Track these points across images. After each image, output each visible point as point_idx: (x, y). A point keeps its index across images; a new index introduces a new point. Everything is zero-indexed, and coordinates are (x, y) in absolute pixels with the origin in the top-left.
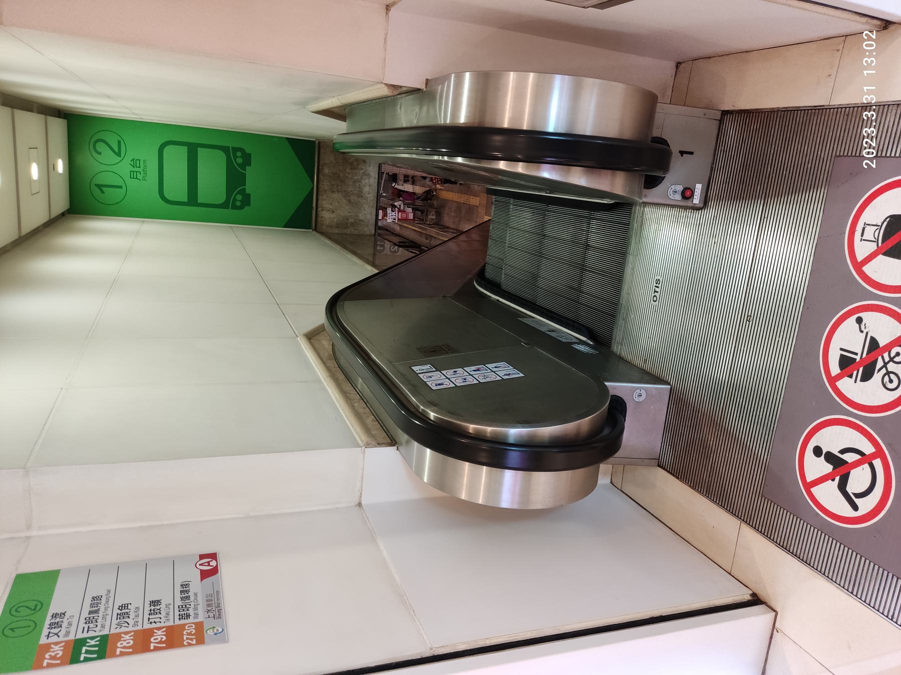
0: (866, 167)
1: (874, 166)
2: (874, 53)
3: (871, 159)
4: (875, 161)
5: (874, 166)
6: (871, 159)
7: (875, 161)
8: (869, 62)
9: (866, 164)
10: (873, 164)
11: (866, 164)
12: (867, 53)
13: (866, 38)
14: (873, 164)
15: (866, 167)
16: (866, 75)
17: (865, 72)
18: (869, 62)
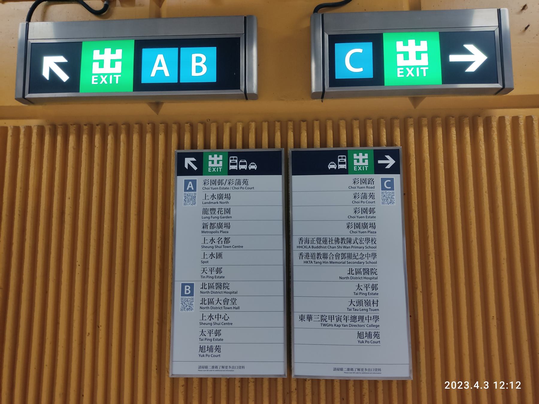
1: (446, 388)
2: (471, 388)
5: (446, 388)
6: (450, 386)
8: (486, 385)
9: (447, 383)
11: (447, 383)
12: (507, 384)
15: (445, 383)
18: (486, 385)
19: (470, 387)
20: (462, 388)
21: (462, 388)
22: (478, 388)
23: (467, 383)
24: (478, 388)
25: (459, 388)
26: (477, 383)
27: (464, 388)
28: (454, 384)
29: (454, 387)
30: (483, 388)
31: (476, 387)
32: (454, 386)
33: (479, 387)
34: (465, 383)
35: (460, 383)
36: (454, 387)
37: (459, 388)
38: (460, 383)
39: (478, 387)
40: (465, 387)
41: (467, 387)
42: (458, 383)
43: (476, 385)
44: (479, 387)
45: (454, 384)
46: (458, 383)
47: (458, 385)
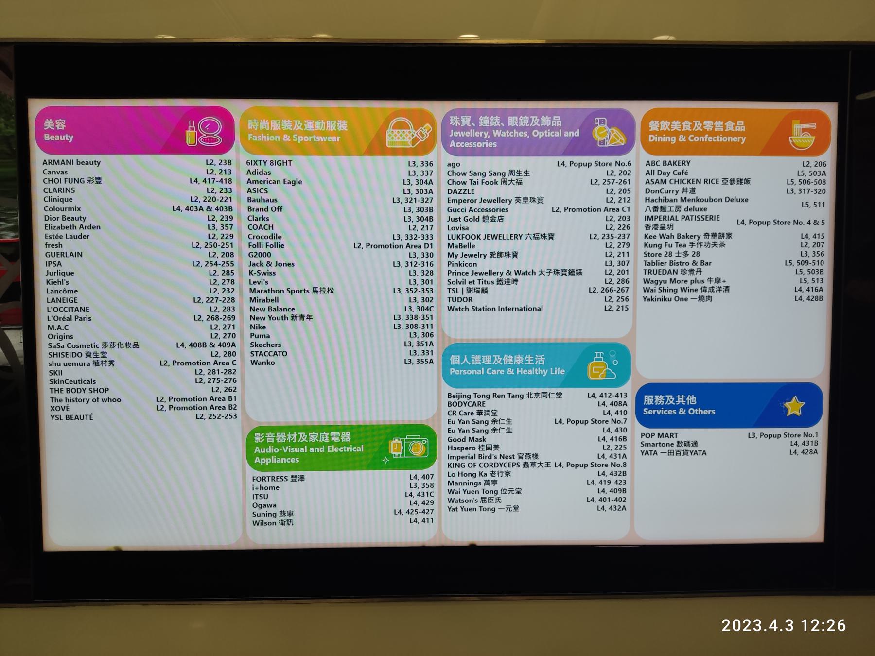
0: (723, 622)
1: (724, 630)
2: (765, 630)
3: (730, 627)
4: (729, 630)
5: (724, 630)
6: (730, 627)
7: (834, 630)
9: (726, 623)
10: (831, 629)
11: (726, 623)
13: (828, 622)
14: (831, 629)
15: (723, 622)
16: (802, 622)
17: (805, 621)
19: (762, 629)
20: (750, 630)
21: (750, 630)
22: (775, 630)
23: (757, 622)
24: (775, 630)
25: (745, 630)
26: (775, 621)
27: (752, 630)
28: (737, 623)
29: (737, 628)
30: (784, 630)
31: (773, 628)
32: (737, 627)
33: (777, 628)
34: (755, 621)
35: (747, 623)
36: (737, 628)
37: (745, 630)
38: (747, 623)
39: (775, 628)
40: (755, 629)
41: (757, 628)
42: (744, 622)
43: (773, 626)
44: (777, 628)
45: (737, 623)
46: (744, 622)
47: (743, 626)
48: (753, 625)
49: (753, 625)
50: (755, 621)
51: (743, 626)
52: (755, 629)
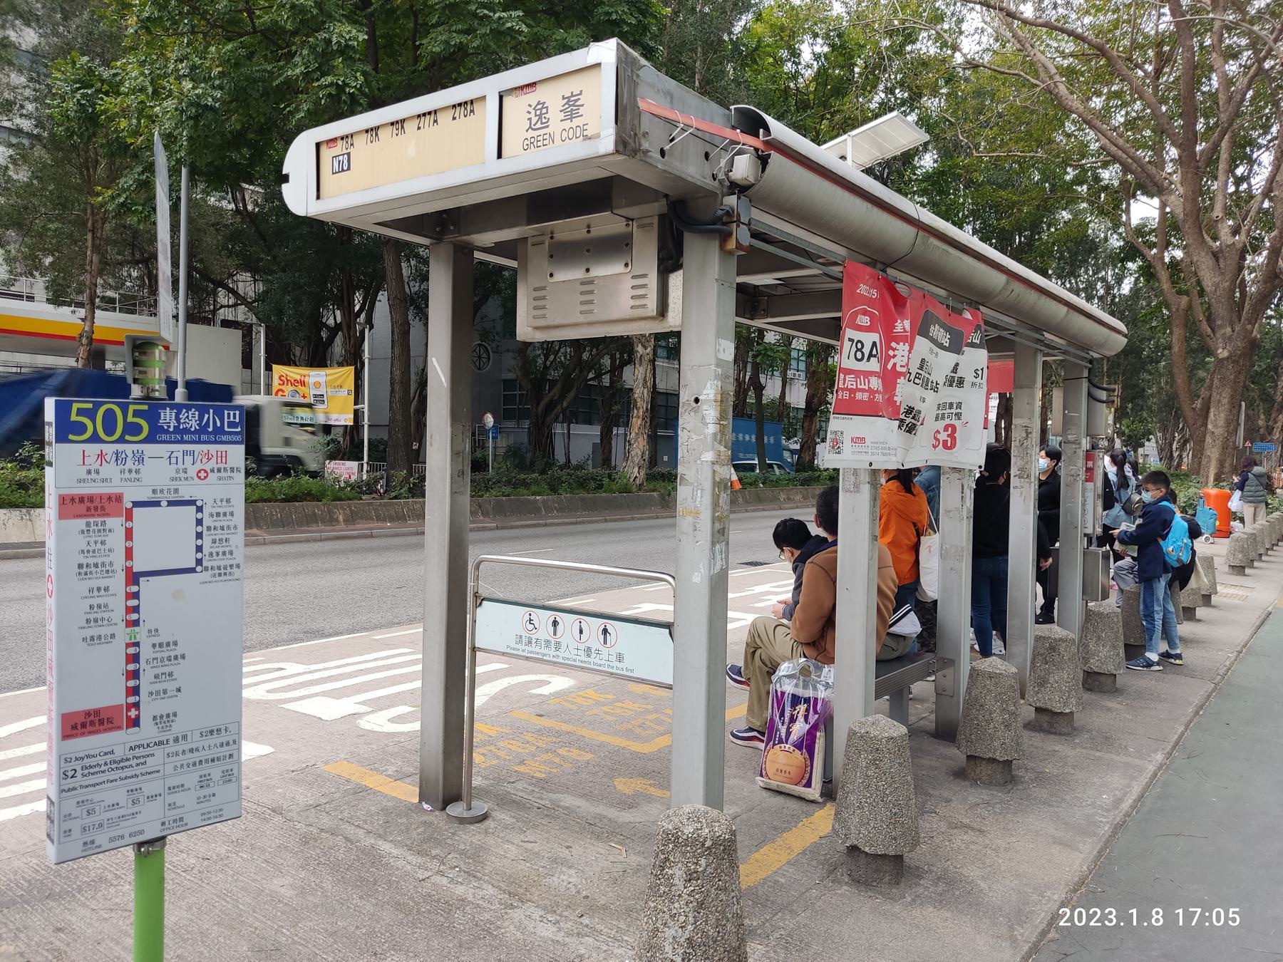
3: (1071, 919)
6: (1071, 919)
23: (1111, 913)
25: (1092, 924)
27: (1104, 924)
28: (1080, 913)
29: (1080, 921)
32: (1080, 920)
34: (1107, 911)
35: (1095, 913)
36: (1080, 921)
37: (1092, 924)
38: (1095, 913)
40: (1106, 922)
41: (1111, 921)
42: (1091, 912)
45: (1080, 913)
46: (1091, 912)
47: (1090, 918)
48: (1104, 917)
49: (1104, 917)
50: (1107, 911)
51: (1090, 918)
52: (1106, 922)
